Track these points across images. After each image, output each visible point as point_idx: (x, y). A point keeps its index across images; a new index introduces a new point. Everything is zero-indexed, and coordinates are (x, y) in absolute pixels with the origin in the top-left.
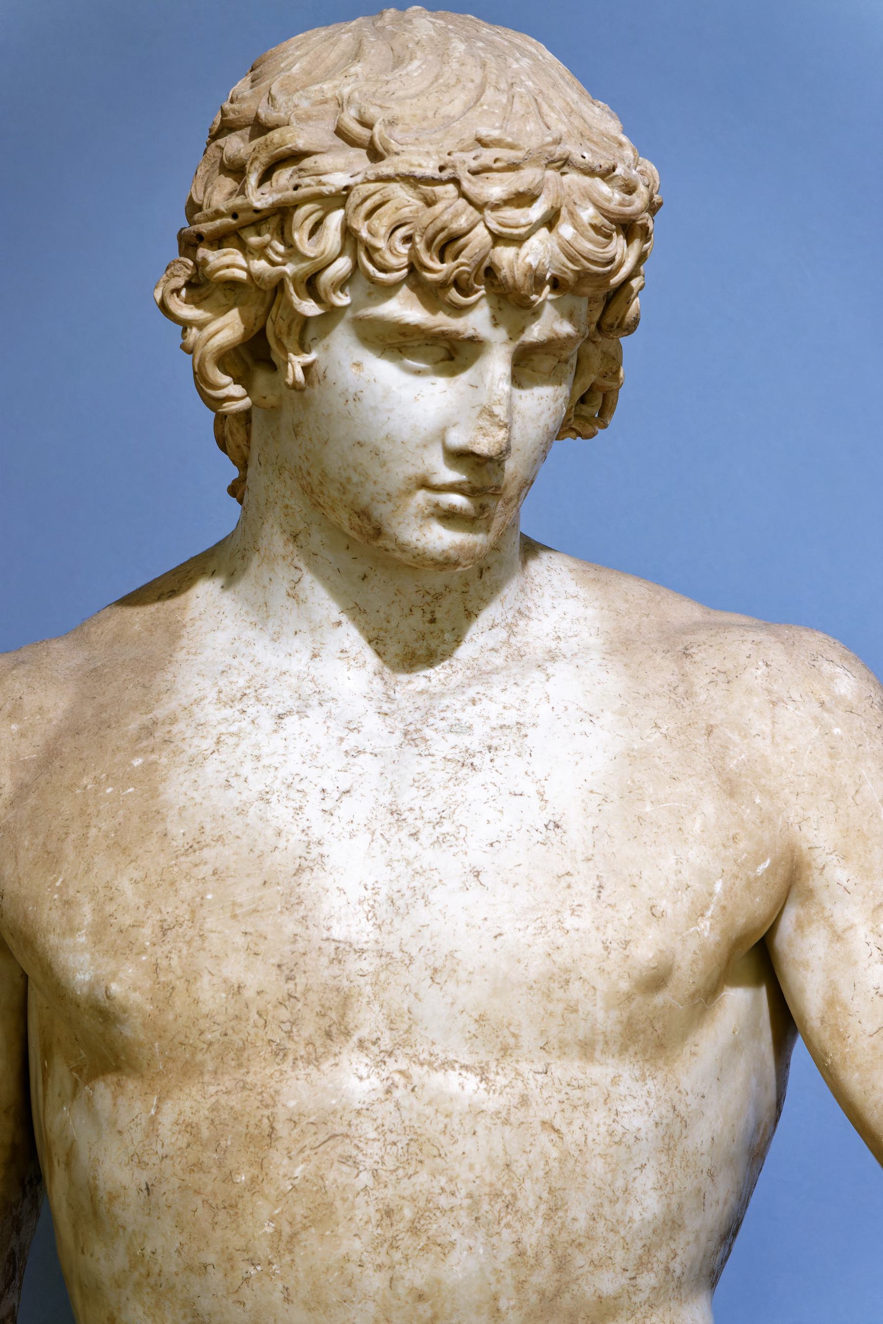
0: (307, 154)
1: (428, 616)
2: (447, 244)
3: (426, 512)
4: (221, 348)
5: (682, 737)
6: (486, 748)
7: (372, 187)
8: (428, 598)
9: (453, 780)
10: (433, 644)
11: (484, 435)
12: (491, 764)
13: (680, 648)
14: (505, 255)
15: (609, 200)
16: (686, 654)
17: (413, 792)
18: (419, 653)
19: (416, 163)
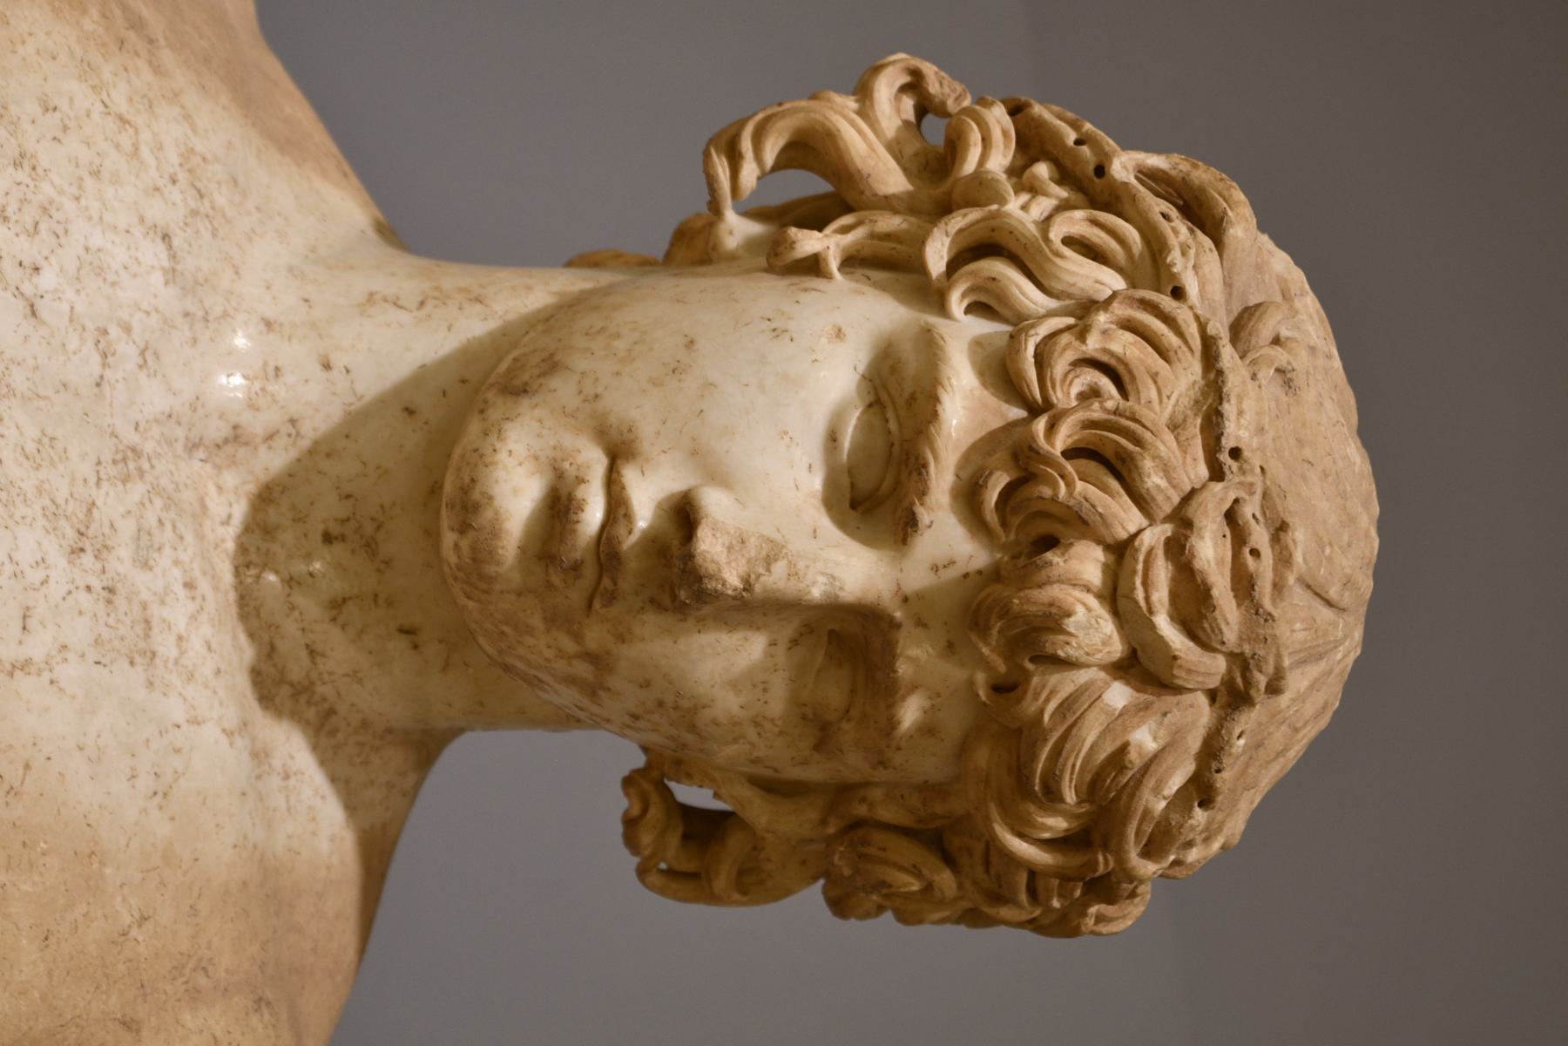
0: (1218, 243)
1: (335, 529)
2: (1110, 455)
3: (566, 465)
4: (831, 136)
5: (122, 967)
6: (110, 583)
7: (1192, 331)
8: (369, 528)
9: (53, 508)
10: (288, 537)
11: (730, 548)
12: (82, 584)
13: (269, 995)
14: (1087, 562)
15: (1157, 790)
16: (260, 1002)
17: (32, 432)
18: (271, 510)
19: (1245, 406)
